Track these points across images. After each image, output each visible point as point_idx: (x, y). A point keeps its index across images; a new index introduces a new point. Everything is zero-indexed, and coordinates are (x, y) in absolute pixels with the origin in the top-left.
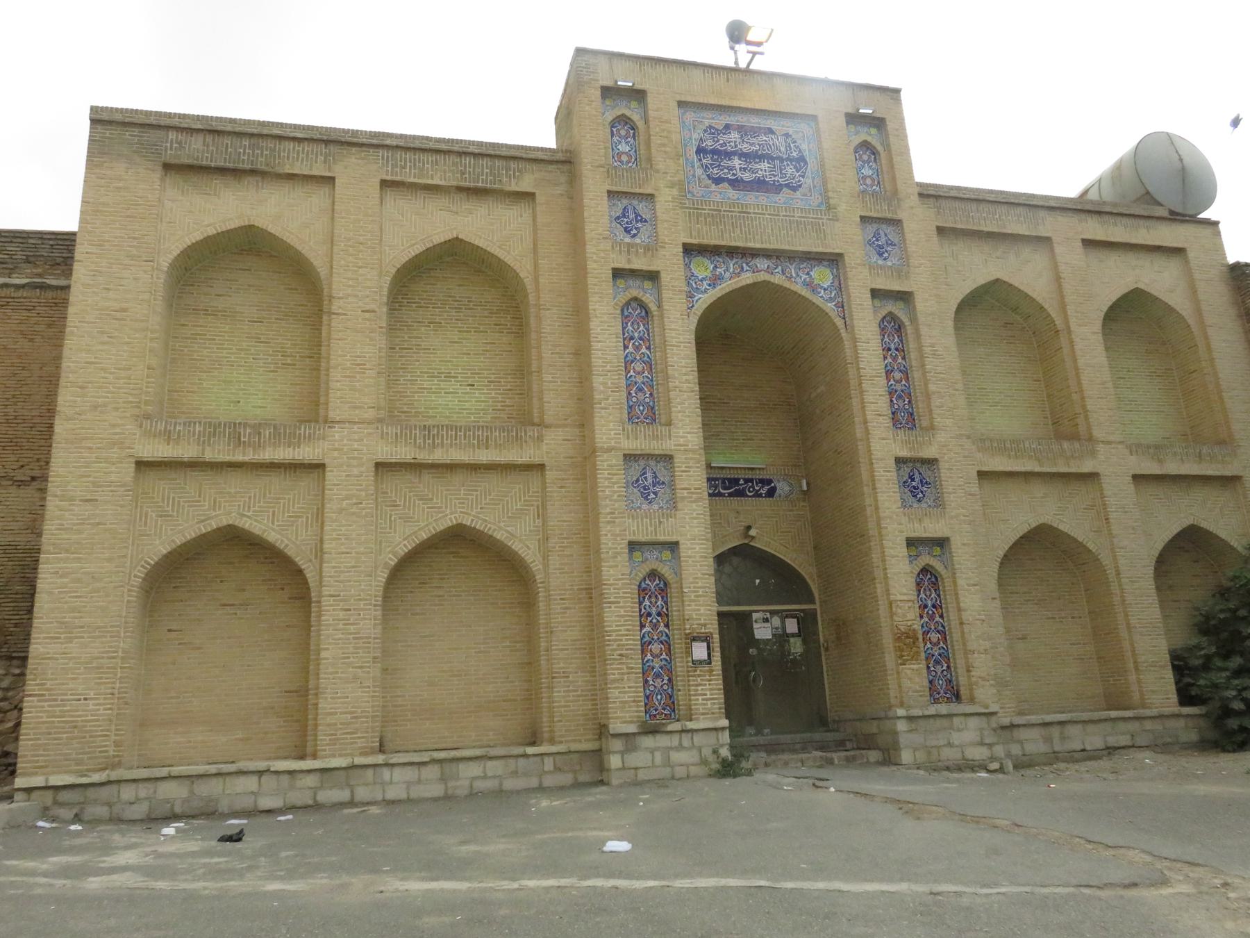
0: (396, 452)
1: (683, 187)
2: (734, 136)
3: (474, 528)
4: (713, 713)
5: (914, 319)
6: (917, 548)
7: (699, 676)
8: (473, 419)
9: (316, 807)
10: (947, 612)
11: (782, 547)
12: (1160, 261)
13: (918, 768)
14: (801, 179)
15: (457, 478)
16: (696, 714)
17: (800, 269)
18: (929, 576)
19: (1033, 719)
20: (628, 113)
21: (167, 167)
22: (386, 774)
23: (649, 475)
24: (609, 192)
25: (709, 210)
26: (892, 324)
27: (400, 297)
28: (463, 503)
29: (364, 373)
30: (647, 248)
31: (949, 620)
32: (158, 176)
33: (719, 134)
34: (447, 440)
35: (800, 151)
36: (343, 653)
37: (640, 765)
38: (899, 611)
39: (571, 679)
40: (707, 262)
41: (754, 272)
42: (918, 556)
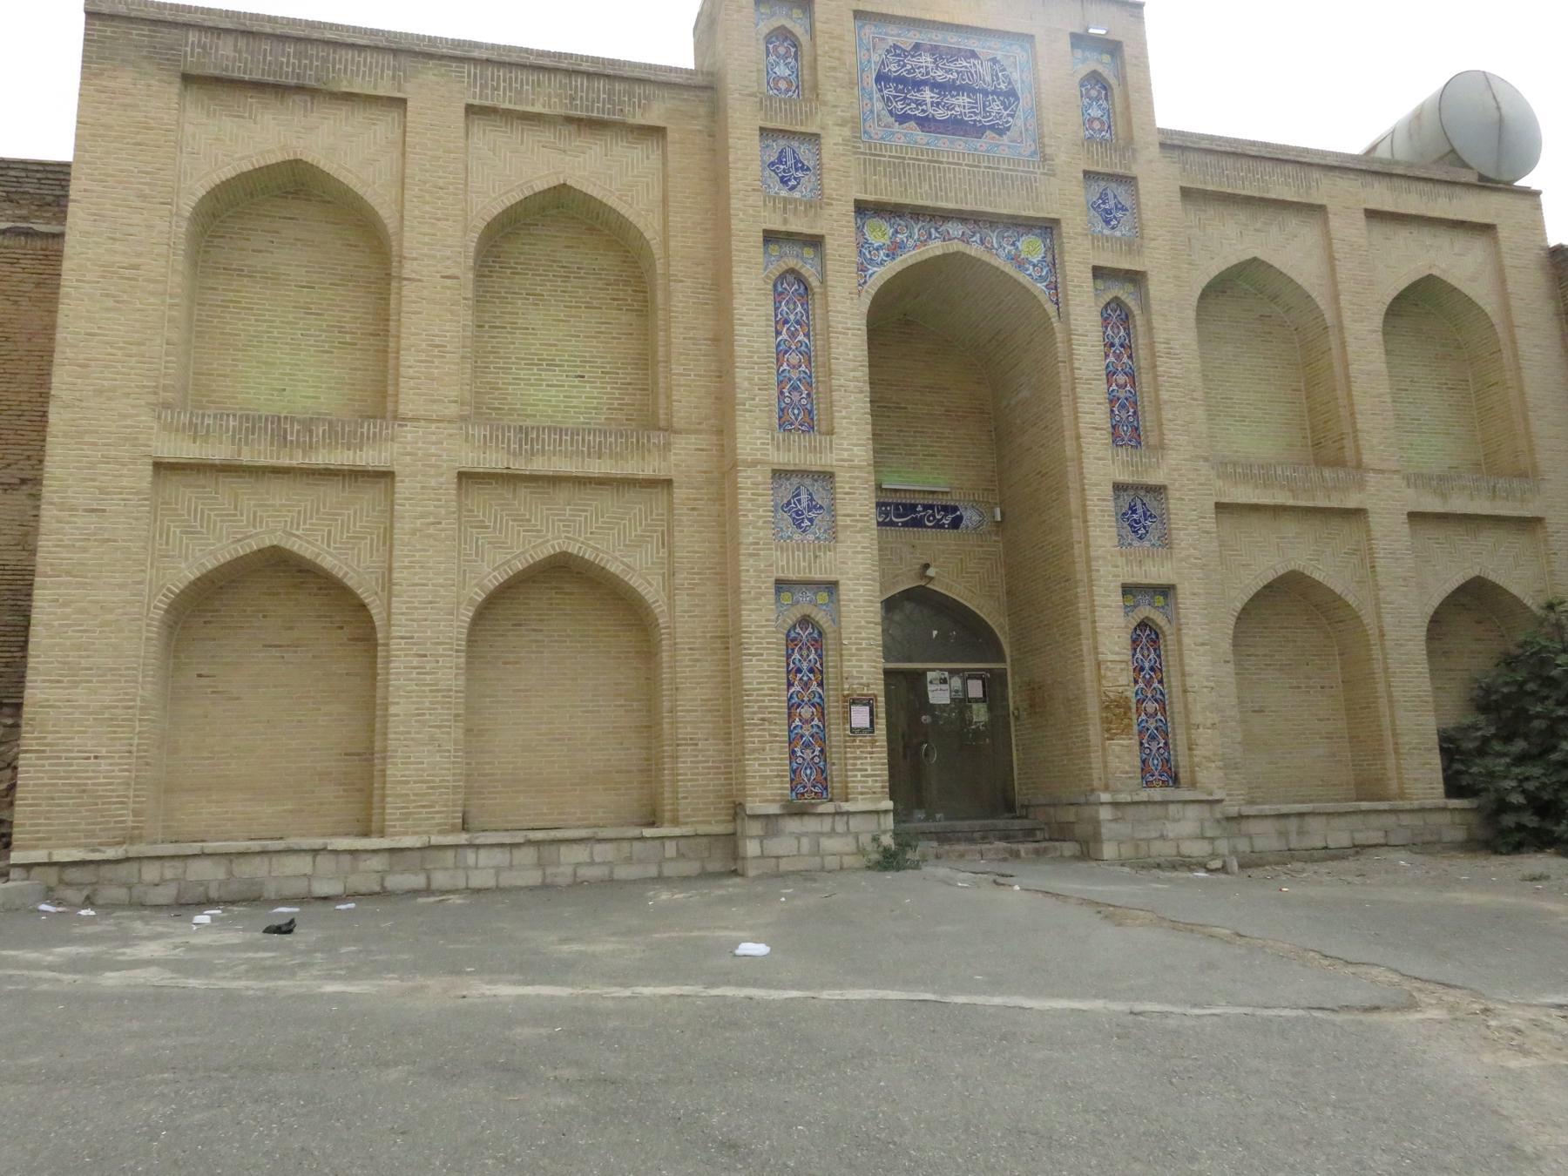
0: (484, 458)
1: (857, 126)
2: (926, 60)
3: (582, 558)
4: (874, 793)
5: (1145, 307)
6: (1134, 596)
7: (859, 747)
8: (582, 420)
9: (383, 894)
10: (1168, 677)
11: (967, 592)
12: (1461, 241)
13: (1122, 865)
14: (1010, 119)
15: (562, 494)
16: (853, 793)
17: (1003, 238)
18: (1148, 632)
19: (1267, 809)
20: (789, 25)
21: (188, 79)
22: (471, 856)
23: (804, 496)
24: (762, 129)
25: (890, 157)
26: (1118, 312)
27: (491, 259)
28: (569, 526)
29: (445, 357)
30: (810, 205)
31: (1170, 687)
32: (177, 91)
33: (906, 57)
34: (549, 445)
35: (1010, 83)
36: (417, 709)
37: (781, 852)
38: (1109, 674)
39: (700, 747)
40: (885, 225)
41: (944, 240)
42: (1135, 607)
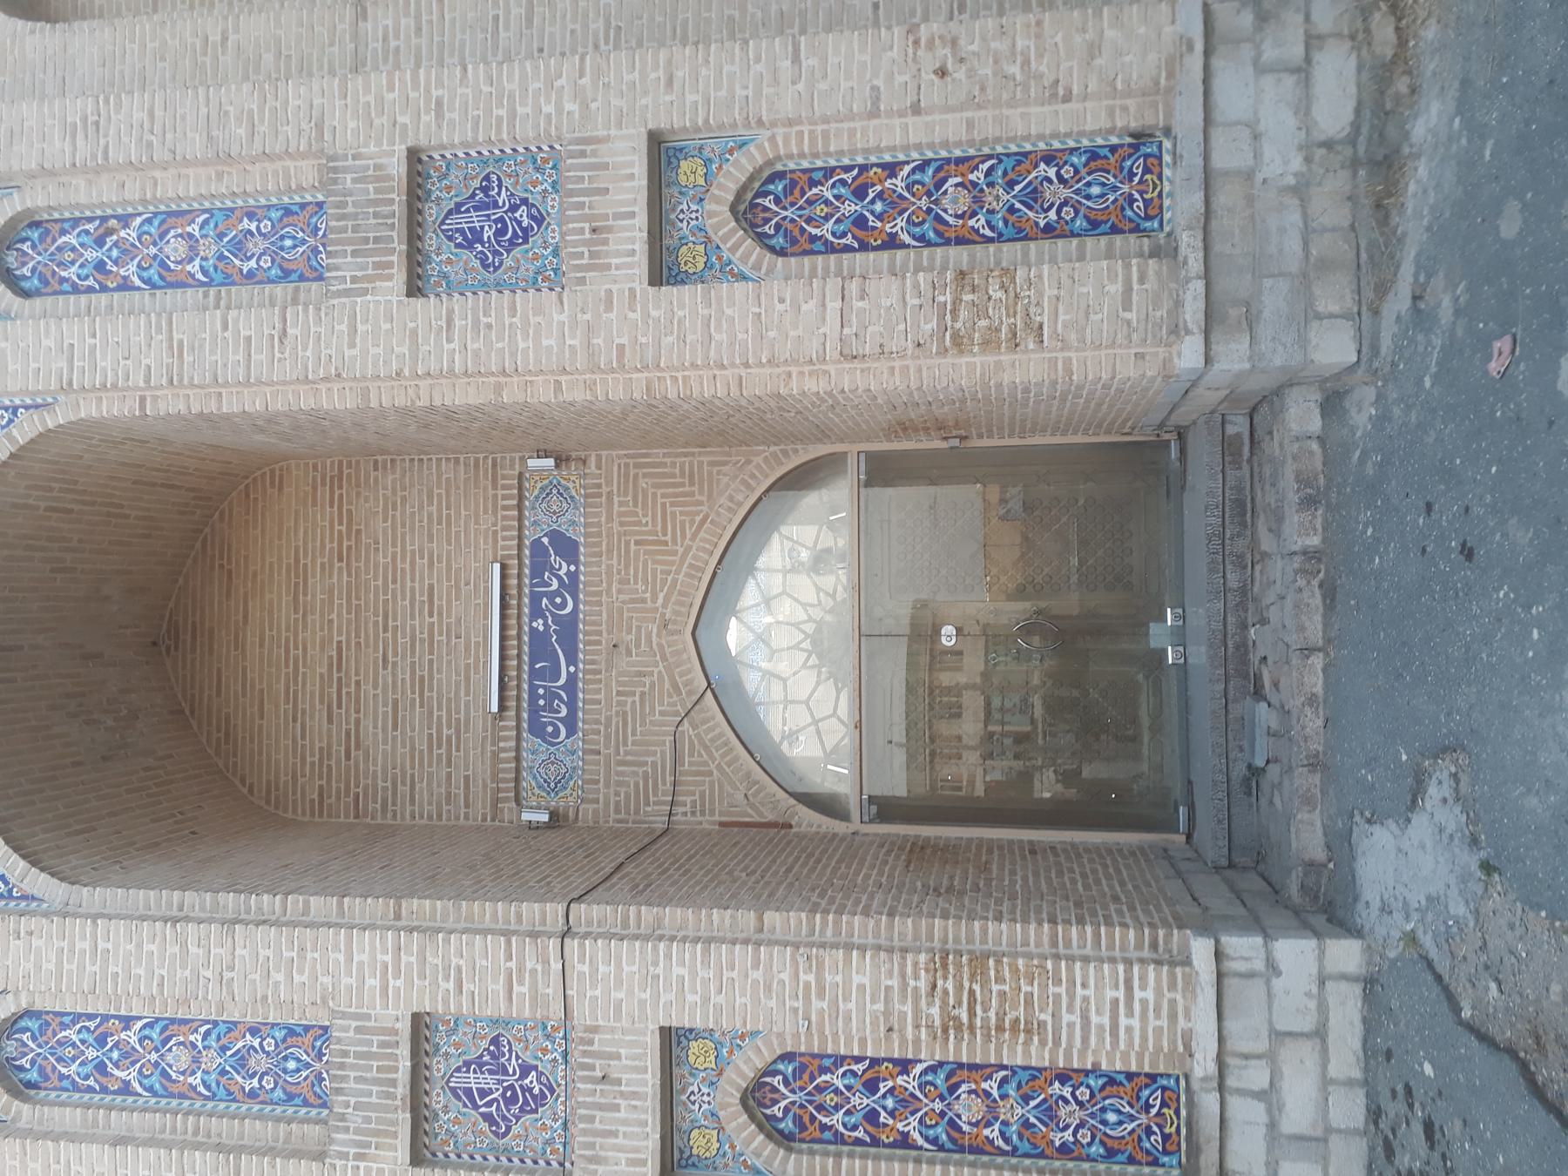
11: (702, 534)
23: (474, 1081)
26: (26, 247)
31: (906, 148)
42: (708, 241)
